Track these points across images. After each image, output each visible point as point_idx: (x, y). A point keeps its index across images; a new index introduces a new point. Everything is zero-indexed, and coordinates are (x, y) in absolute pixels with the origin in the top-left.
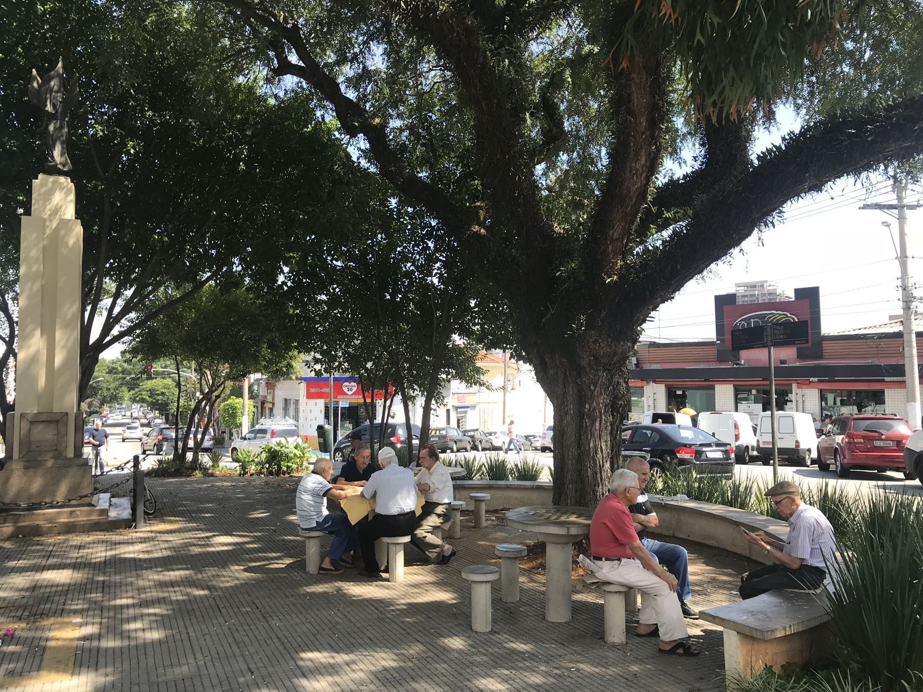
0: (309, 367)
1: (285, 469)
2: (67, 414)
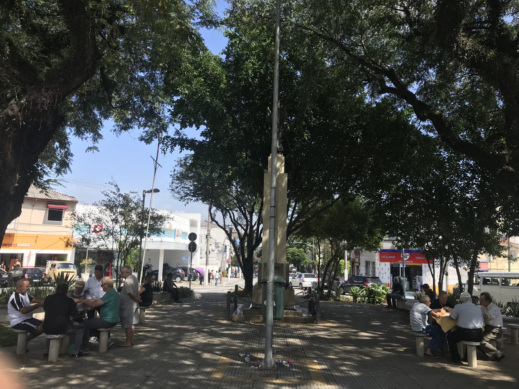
0: (394, 244)
1: (378, 300)
2: (283, 264)
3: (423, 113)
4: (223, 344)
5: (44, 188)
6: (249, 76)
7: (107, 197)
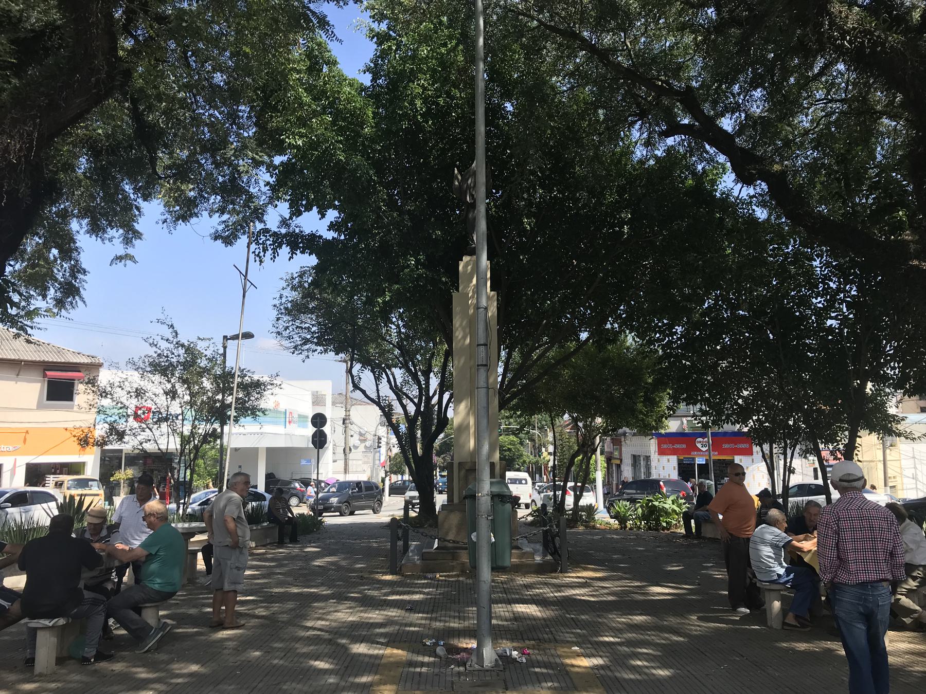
1: (664, 524)
3: (749, 170)
4: (389, 622)
5: (22, 328)
6: (417, 111)
7: (154, 349)
